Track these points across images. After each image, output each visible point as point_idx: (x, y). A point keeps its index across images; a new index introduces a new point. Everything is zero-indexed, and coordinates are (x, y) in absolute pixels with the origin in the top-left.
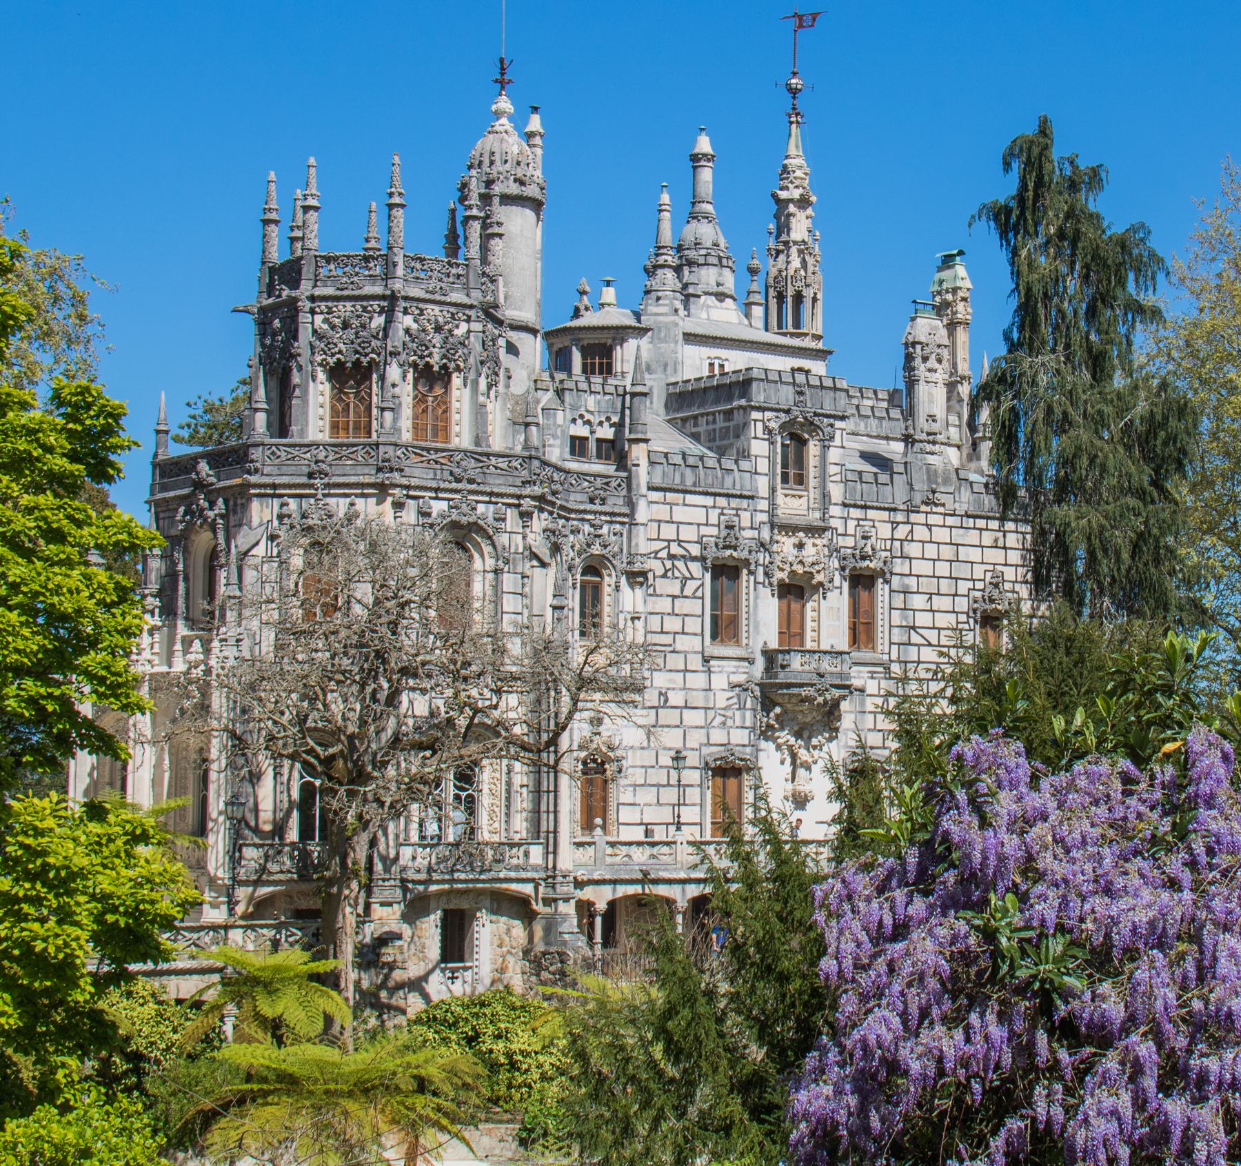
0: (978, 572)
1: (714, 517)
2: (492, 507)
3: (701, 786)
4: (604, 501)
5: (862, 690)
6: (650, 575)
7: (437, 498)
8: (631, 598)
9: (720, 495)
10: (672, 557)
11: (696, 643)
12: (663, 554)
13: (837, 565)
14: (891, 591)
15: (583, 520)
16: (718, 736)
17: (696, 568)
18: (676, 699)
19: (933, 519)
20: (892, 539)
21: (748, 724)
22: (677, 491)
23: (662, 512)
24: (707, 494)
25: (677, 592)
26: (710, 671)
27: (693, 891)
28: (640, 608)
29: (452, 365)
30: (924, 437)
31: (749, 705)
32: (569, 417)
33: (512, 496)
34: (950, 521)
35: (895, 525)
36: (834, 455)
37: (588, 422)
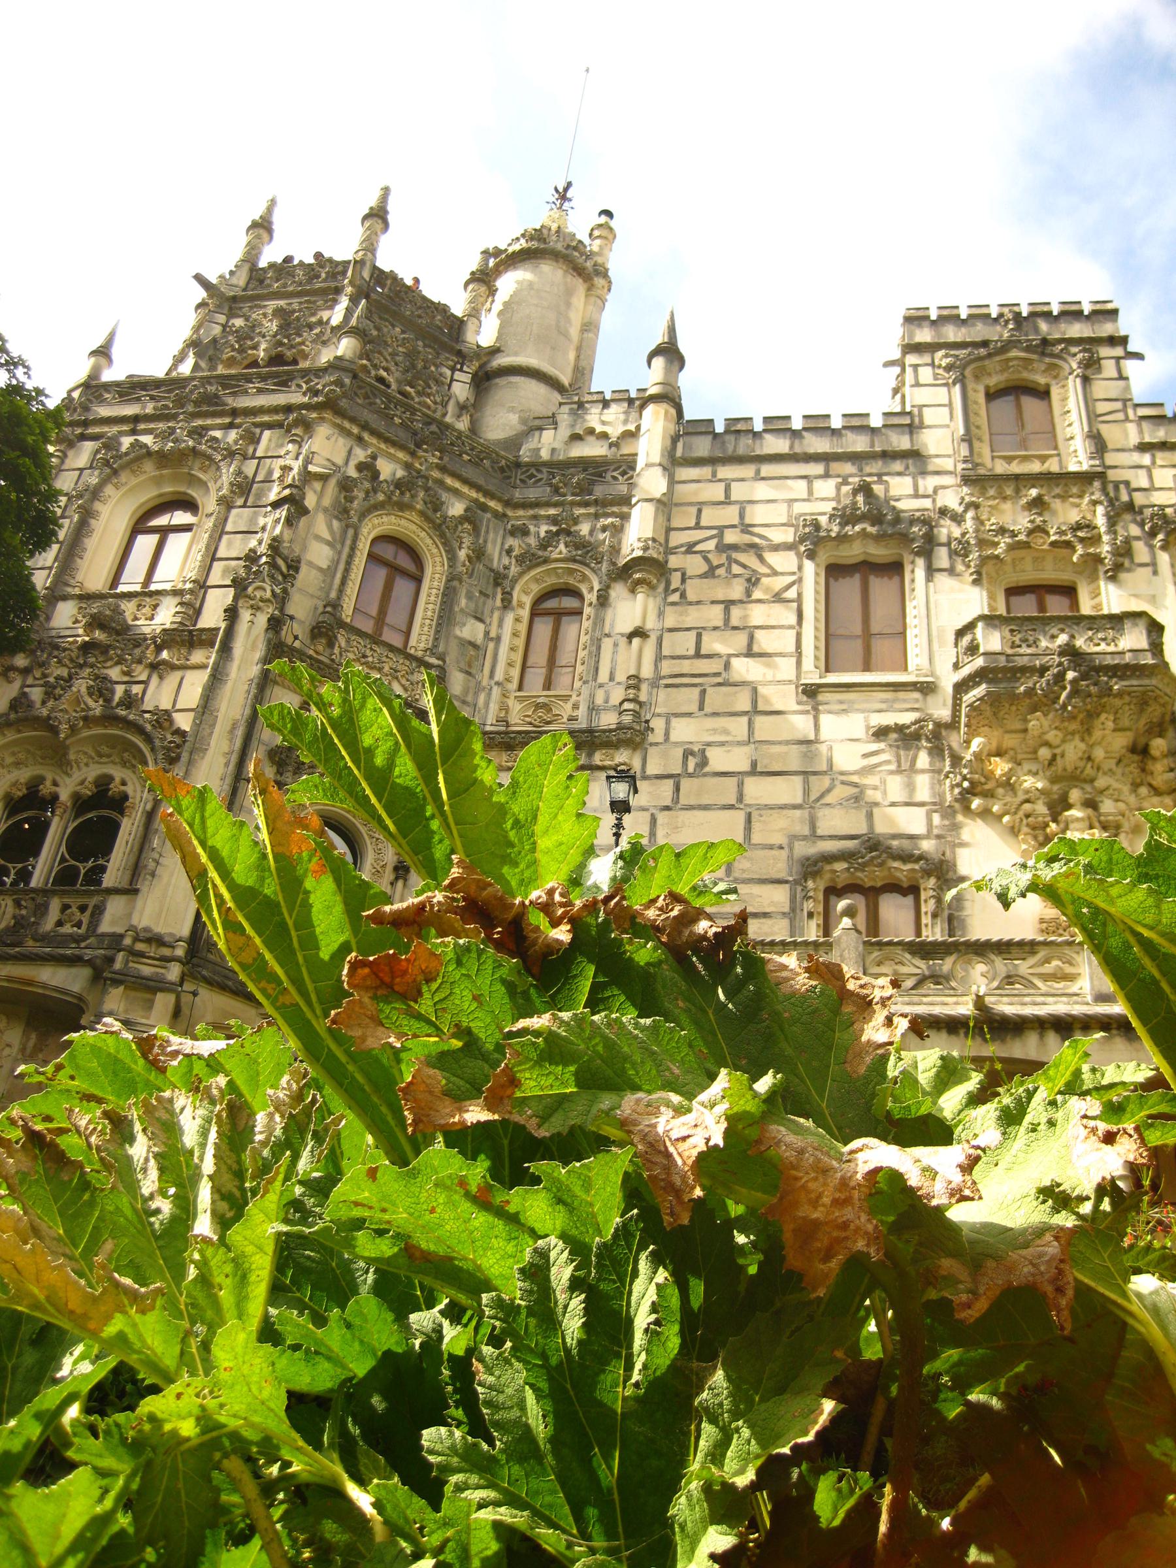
7: (134, 432)
8: (630, 609)
10: (722, 548)
11: (786, 669)
12: (711, 545)
13: (1135, 530)
15: (535, 517)
16: (839, 822)
17: (784, 561)
18: (718, 760)
25: (736, 591)
28: (651, 624)
29: (289, 354)
32: (564, 432)
33: (275, 410)
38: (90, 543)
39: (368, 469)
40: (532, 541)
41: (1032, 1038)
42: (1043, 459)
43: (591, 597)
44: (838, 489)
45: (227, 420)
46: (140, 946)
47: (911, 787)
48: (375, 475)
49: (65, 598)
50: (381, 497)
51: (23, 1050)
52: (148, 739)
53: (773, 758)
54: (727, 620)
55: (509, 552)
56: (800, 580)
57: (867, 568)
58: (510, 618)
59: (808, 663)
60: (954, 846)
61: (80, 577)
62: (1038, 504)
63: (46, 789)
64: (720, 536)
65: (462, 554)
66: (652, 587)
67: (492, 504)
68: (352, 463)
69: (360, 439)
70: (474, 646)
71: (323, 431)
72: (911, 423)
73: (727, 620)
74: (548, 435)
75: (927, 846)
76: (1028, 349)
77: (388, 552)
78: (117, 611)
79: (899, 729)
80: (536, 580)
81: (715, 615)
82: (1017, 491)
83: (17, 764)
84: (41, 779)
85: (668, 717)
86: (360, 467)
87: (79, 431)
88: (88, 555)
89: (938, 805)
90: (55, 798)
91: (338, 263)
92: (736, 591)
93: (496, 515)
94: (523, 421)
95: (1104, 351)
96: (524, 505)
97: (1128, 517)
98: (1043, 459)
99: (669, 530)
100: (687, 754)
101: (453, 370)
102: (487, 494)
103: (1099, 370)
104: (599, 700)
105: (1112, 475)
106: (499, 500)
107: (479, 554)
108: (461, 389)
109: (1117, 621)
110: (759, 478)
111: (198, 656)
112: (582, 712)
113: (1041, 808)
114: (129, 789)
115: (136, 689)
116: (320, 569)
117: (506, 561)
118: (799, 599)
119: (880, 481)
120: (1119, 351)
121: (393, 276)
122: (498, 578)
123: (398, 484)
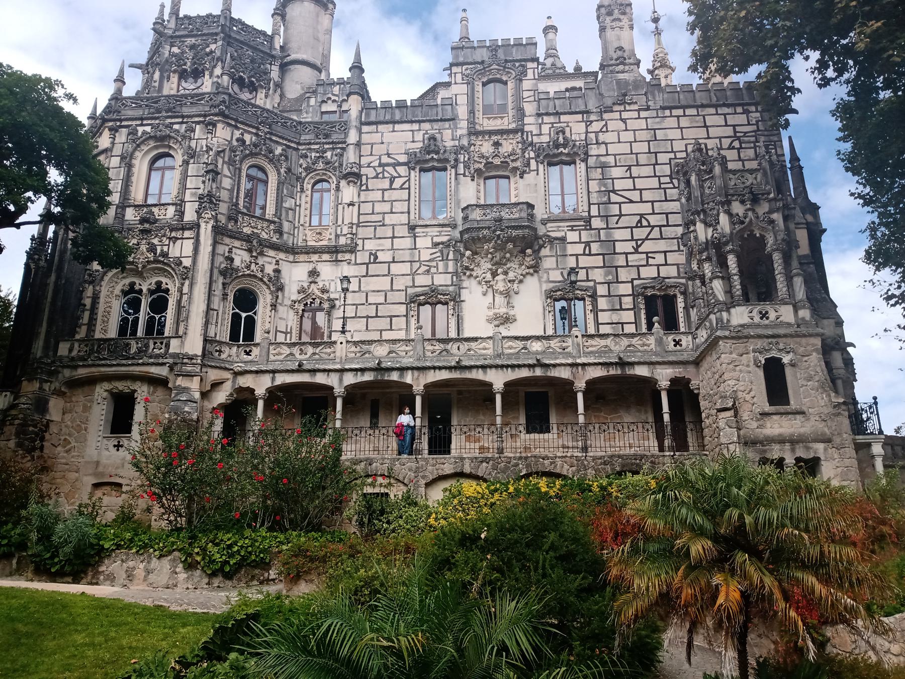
0: (679, 146)
1: (419, 136)
2: (184, 126)
3: (406, 316)
4: (327, 136)
5: (563, 239)
6: (364, 178)
7: (142, 125)
8: (349, 192)
9: (424, 121)
11: (404, 219)
12: (376, 163)
13: (532, 155)
14: (587, 168)
15: (310, 149)
16: (423, 280)
17: (402, 170)
18: (382, 257)
19: (625, 115)
20: (587, 132)
21: (451, 269)
22: (387, 123)
23: (376, 138)
24: (412, 122)
26: (415, 237)
27: (350, 379)
28: (356, 199)
30: (613, 62)
31: (451, 256)
32: (319, 100)
34: (643, 114)
35: (589, 123)
36: (526, 85)
37: (334, 101)
38: (134, 179)
39: (241, 141)
40: (309, 160)
41: (474, 371)
42: (502, 118)
43: (333, 186)
44: (424, 135)
45: (180, 120)
46: (185, 361)
47: (447, 266)
48: (244, 142)
49: (129, 206)
50: (247, 152)
51: (149, 393)
52: (173, 269)
53: (399, 256)
54: (383, 197)
55: (301, 166)
56: (409, 180)
57: (433, 169)
58: (304, 195)
59: (412, 217)
60: (460, 288)
61: (133, 195)
62: (497, 144)
63: (137, 287)
64: (380, 159)
65: (282, 171)
66: (356, 183)
67: (293, 145)
68: (234, 138)
69: (237, 128)
70: (291, 209)
71: (220, 126)
72: (451, 103)
73: (383, 197)
74: (312, 101)
75: (451, 289)
76: (498, 65)
77: (254, 172)
78: (152, 213)
79: (442, 243)
80: (312, 178)
81: (378, 195)
82: (490, 137)
83: (124, 278)
84: (134, 283)
85: (364, 239)
86: (238, 140)
87: (118, 124)
88: (134, 185)
89: (456, 273)
90: (141, 290)
91: (214, 17)
92: (386, 185)
93: (294, 149)
94: (303, 88)
95: (530, 65)
96: (304, 144)
97: (530, 148)
98: (502, 118)
99: (360, 156)
100: (371, 254)
101: (271, 64)
102: (289, 141)
103: (526, 75)
104: (339, 233)
105: (527, 128)
106: (295, 142)
107: (289, 170)
108: (275, 73)
109: (517, 204)
110: (394, 131)
111: (187, 234)
112: (333, 237)
113: (489, 276)
114: (169, 287)
115: (165, 248)
116: (228, 190)
117: (300, 170)
118: (409, 188)
119: (439, 133)
120: (535, 65)
121: (240, 21)
122: (298, 179)
123: (255, 145)
